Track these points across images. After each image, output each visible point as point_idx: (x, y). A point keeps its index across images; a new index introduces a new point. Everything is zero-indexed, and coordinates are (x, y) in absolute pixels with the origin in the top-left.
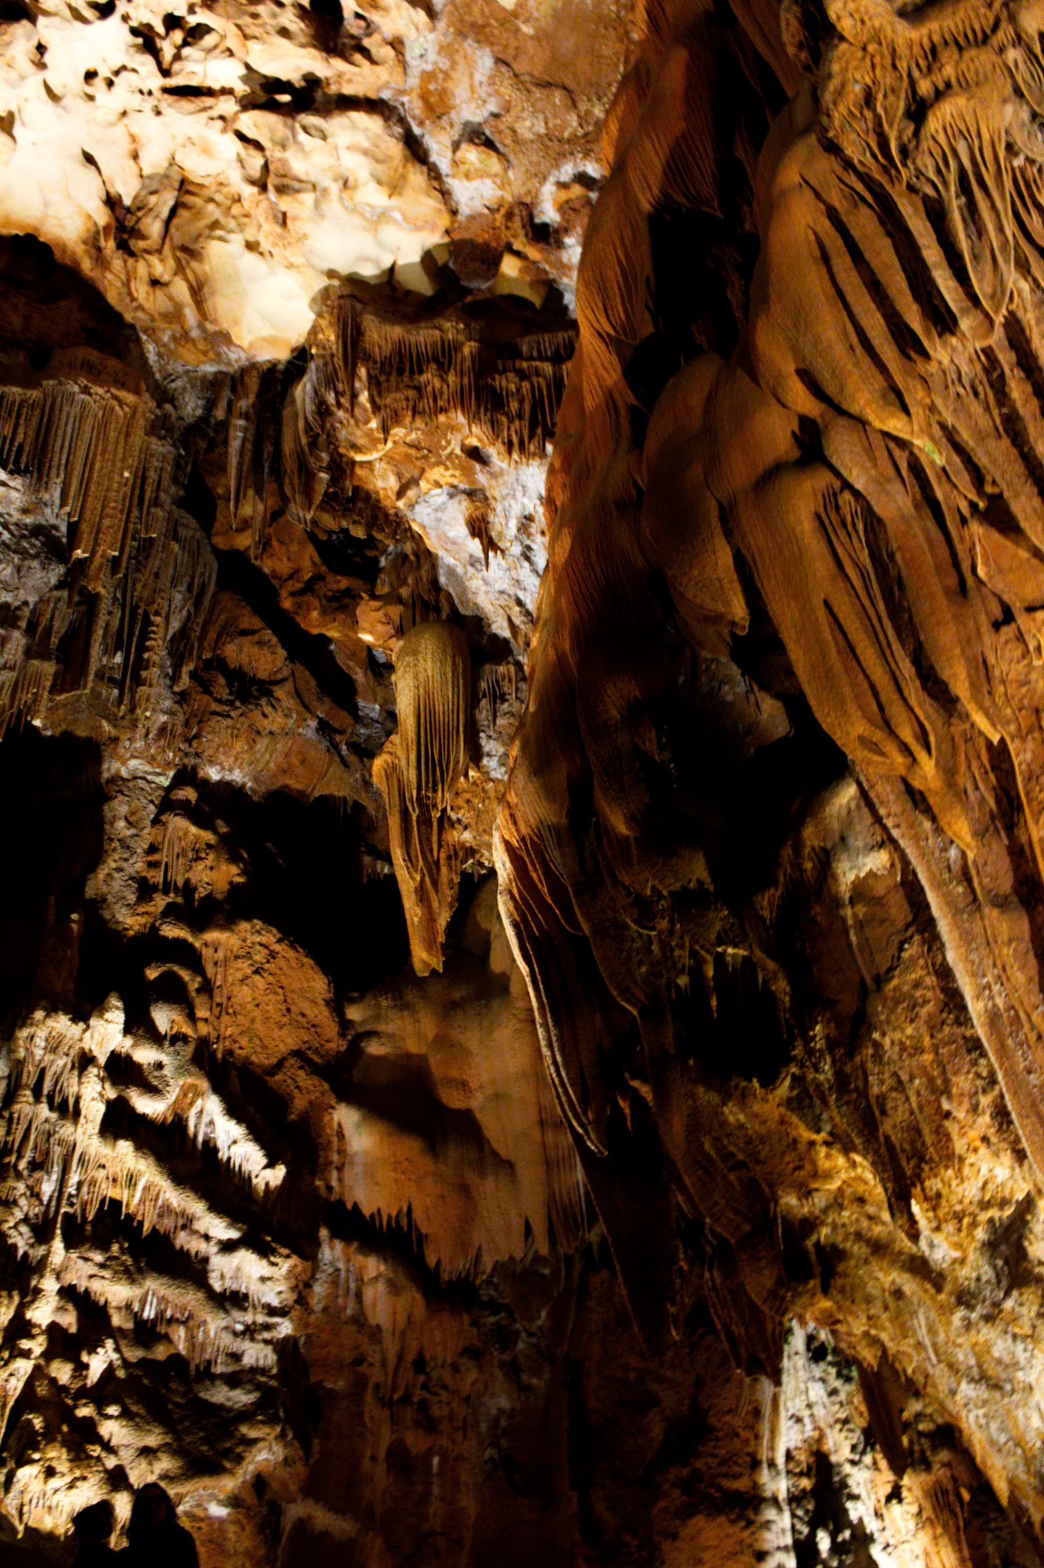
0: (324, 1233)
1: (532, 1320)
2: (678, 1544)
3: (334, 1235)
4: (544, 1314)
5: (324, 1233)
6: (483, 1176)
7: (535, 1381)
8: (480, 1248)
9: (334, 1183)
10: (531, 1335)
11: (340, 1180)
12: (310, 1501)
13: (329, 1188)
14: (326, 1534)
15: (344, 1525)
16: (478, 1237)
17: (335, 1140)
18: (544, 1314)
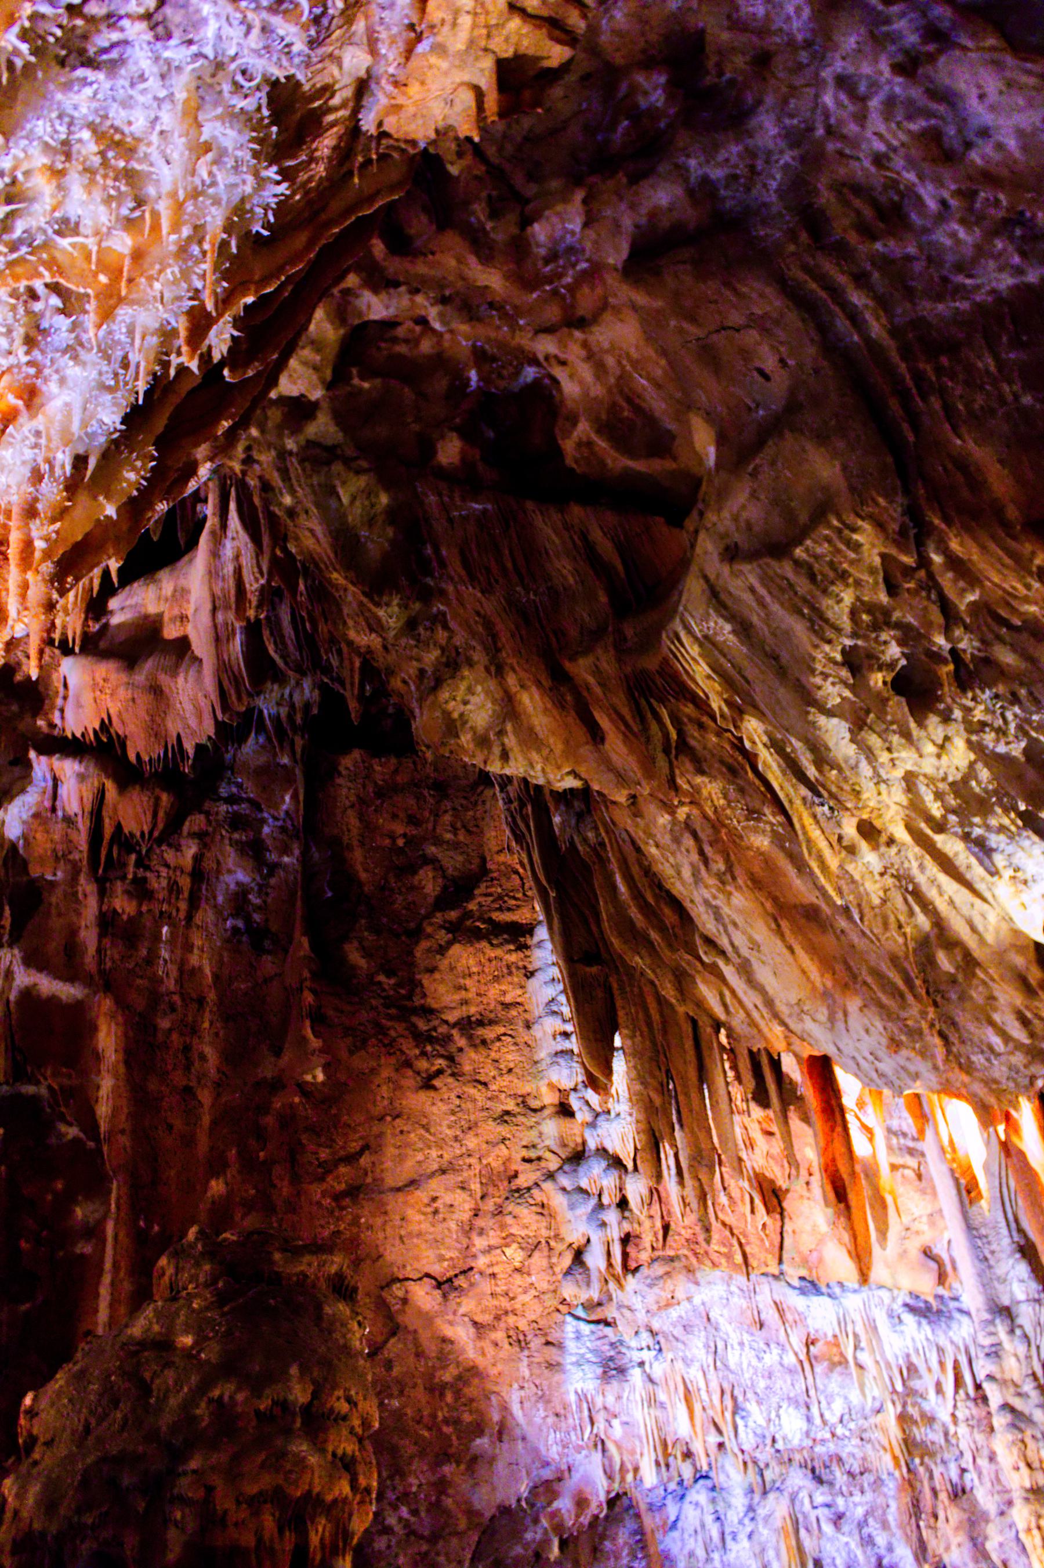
0: (32, 754)
1: (276, 806)
2: (437, 976)
3: (40, 752)
4: (287, 798)
5: (32, 754)
6: (174, 675)
7: (286, 859)
8: (179, 736)
9: (57, 721)
10: (276, 819)
11: (63, 718)
12: (32, 971)
13: (52, 726)
14: (53, 999)
15: (72, 991)
16: (173, 727)
17: (61, 689)
18: (287, 798)
